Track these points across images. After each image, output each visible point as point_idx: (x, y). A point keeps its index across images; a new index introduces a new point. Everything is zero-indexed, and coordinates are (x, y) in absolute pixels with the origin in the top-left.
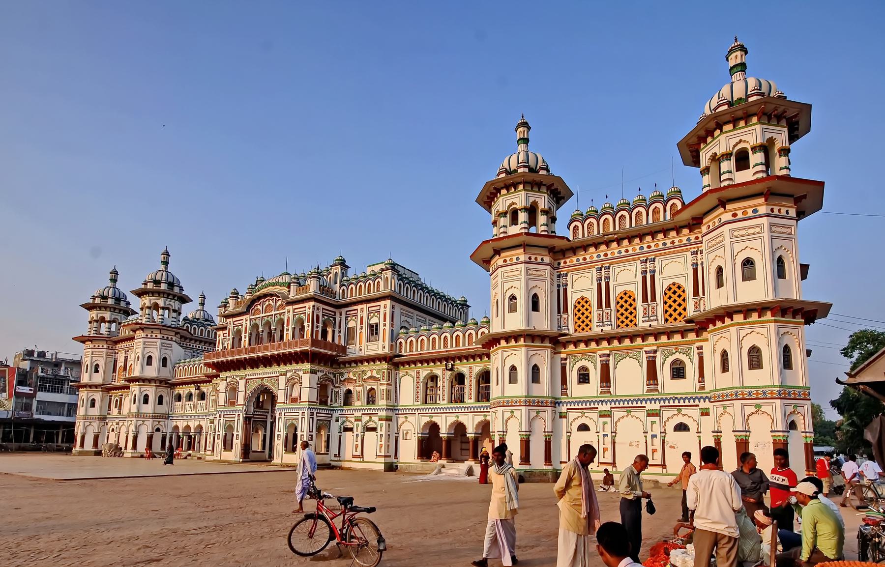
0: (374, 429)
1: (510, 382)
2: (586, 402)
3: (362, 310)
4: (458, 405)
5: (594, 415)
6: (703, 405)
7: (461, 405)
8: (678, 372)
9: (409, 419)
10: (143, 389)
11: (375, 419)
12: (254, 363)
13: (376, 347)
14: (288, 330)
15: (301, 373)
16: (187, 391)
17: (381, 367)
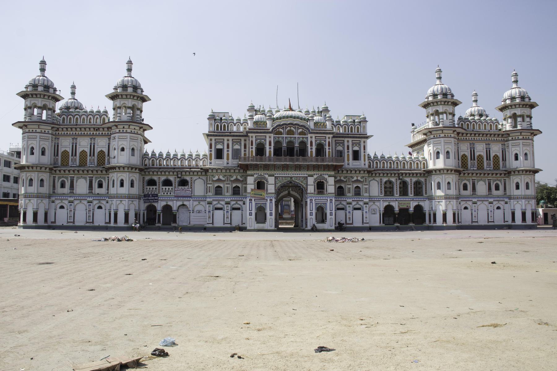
0: (359, 209)
3: (348, 141)
5: (470, 203)
6: (506, 200)
8: (497, 188)
10: (131, 175)
11: (361, 203)
12: (285, 168)
13: (359, 164)
14: (311, 149)
15: (326, 177)
16: (163, 178)
17: (364, 175)
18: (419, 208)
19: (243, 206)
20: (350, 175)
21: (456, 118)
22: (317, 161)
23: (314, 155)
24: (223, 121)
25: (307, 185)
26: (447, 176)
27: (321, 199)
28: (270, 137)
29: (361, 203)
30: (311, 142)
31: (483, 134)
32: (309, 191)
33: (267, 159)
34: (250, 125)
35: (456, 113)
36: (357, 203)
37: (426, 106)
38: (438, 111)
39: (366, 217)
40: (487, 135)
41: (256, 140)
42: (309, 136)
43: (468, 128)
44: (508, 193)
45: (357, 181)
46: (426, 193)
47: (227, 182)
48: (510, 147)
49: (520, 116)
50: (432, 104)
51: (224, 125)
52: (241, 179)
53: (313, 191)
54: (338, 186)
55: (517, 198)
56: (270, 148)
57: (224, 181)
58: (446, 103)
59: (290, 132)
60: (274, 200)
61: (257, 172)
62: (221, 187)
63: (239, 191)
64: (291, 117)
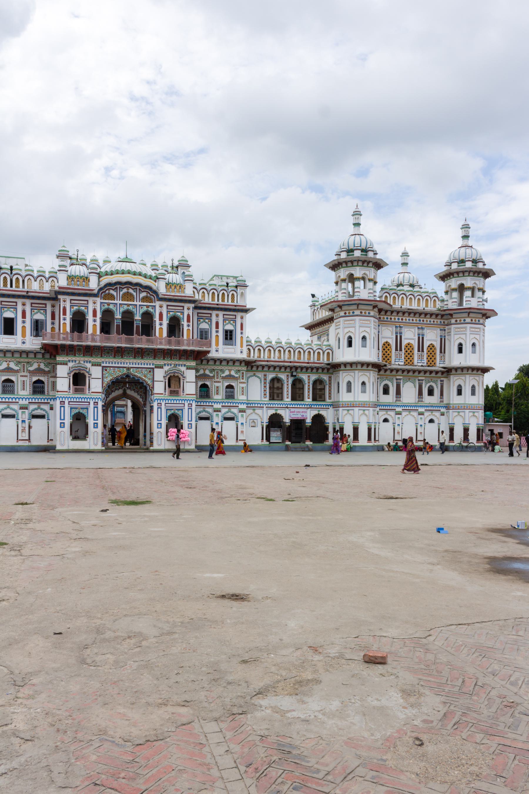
0: (232, 419)
1: (362, 392)
2: (390, 406)
3: (217, 316)
4: (300, 403)
5: (392, 413)
6: (443, 410)
7: (302, 403)
9: (257, 411)
11: (235, 411)
12: (119, 352)
14: (161, 324)
15: (183, 369)
17: (240, 368)
18: (318, 419)
19: (51, 412)
20: (220, 368)
21: (378, 288)
22: (169, 343)
23: (165, 334)
24: (14, 272)
25: (153, 381)
26: (360, 374)
27: (174, 403)
28: (95, 303)
29: (235, 411)
30: (161, 315)
31: (415, 314)
32: (156, 391)
33: (90, 337)
34: (63, 281)
35: (378, 280)
36: (229, 411)
37: (335, 266)
38: (352, 275)
39: (242, 432)
40: (420, 314)
41: (71, 306)
42: (157, 304)
43: (394, 302)
44: (445, 401)
45: (230, 377)
46: (330, 397)
47: (23, 374)
48: (452, 333)
49: (469, 288)
50: (344, 265)
51: (17, 278)
52: (47, 369)
53: (162, 391)
54: (200, 383)
55: (459, 408)
56: (95, 321)
57: (17, 371)
58: (365, 264)
59: (128, 297)
60: (100, 404)
61: (74, 359)
62: (11, 381)
63: (43, 387)
64: (129, 272)
